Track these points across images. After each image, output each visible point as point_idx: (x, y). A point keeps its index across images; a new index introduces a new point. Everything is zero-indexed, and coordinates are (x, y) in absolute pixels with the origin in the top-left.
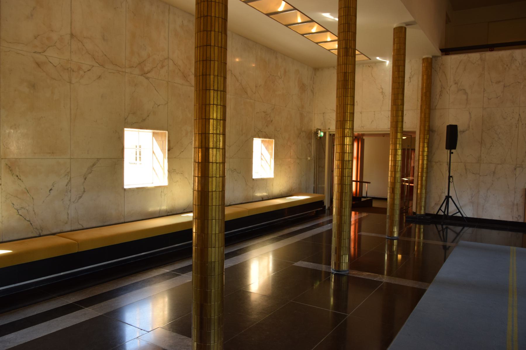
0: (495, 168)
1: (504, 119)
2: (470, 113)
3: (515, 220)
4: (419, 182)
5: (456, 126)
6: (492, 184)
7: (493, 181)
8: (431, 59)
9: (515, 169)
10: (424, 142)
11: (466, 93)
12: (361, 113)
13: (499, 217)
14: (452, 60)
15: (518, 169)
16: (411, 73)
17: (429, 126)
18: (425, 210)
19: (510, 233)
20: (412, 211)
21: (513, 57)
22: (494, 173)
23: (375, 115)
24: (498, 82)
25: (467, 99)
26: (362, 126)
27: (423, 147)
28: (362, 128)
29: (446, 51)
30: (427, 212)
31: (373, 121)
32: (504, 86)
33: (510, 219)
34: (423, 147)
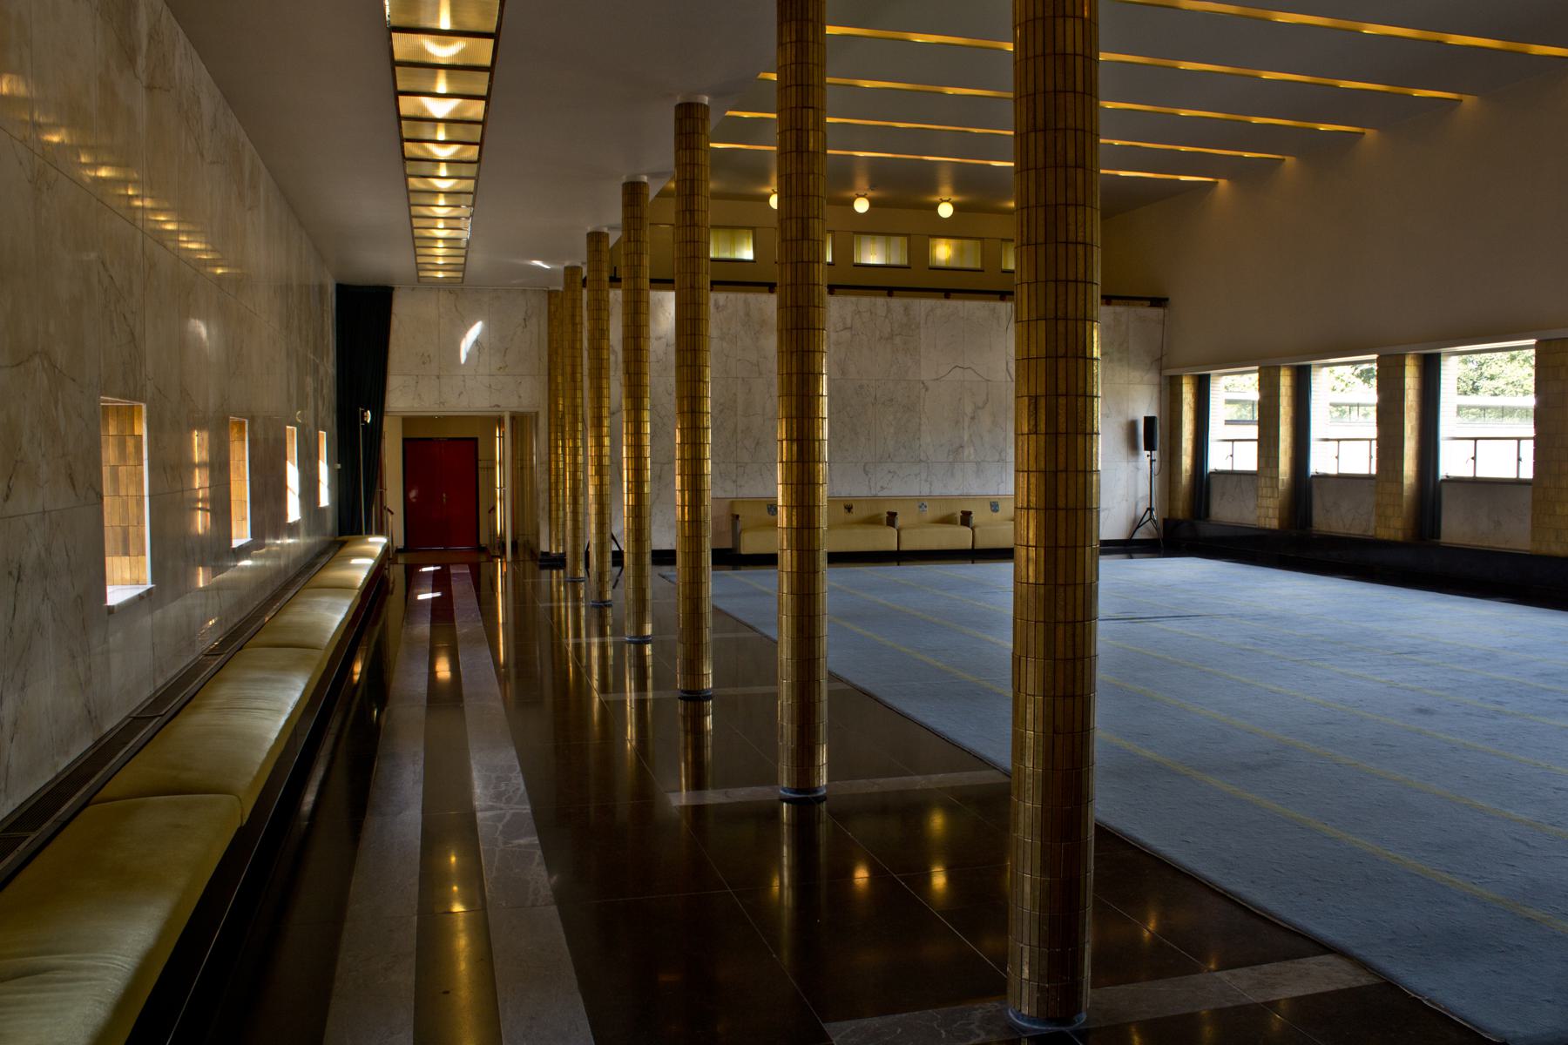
0: (661, 470)
4: (554, 499)
6: (658, 495)
7: (659, 490)
12: (438, 377)
13: (671, 544)
16: (526, 313)
20: (452, 564)
22: (660, 477)
23: (464, 381)
26: (441, 403)
28: (441, 405)
31: (462, 393)
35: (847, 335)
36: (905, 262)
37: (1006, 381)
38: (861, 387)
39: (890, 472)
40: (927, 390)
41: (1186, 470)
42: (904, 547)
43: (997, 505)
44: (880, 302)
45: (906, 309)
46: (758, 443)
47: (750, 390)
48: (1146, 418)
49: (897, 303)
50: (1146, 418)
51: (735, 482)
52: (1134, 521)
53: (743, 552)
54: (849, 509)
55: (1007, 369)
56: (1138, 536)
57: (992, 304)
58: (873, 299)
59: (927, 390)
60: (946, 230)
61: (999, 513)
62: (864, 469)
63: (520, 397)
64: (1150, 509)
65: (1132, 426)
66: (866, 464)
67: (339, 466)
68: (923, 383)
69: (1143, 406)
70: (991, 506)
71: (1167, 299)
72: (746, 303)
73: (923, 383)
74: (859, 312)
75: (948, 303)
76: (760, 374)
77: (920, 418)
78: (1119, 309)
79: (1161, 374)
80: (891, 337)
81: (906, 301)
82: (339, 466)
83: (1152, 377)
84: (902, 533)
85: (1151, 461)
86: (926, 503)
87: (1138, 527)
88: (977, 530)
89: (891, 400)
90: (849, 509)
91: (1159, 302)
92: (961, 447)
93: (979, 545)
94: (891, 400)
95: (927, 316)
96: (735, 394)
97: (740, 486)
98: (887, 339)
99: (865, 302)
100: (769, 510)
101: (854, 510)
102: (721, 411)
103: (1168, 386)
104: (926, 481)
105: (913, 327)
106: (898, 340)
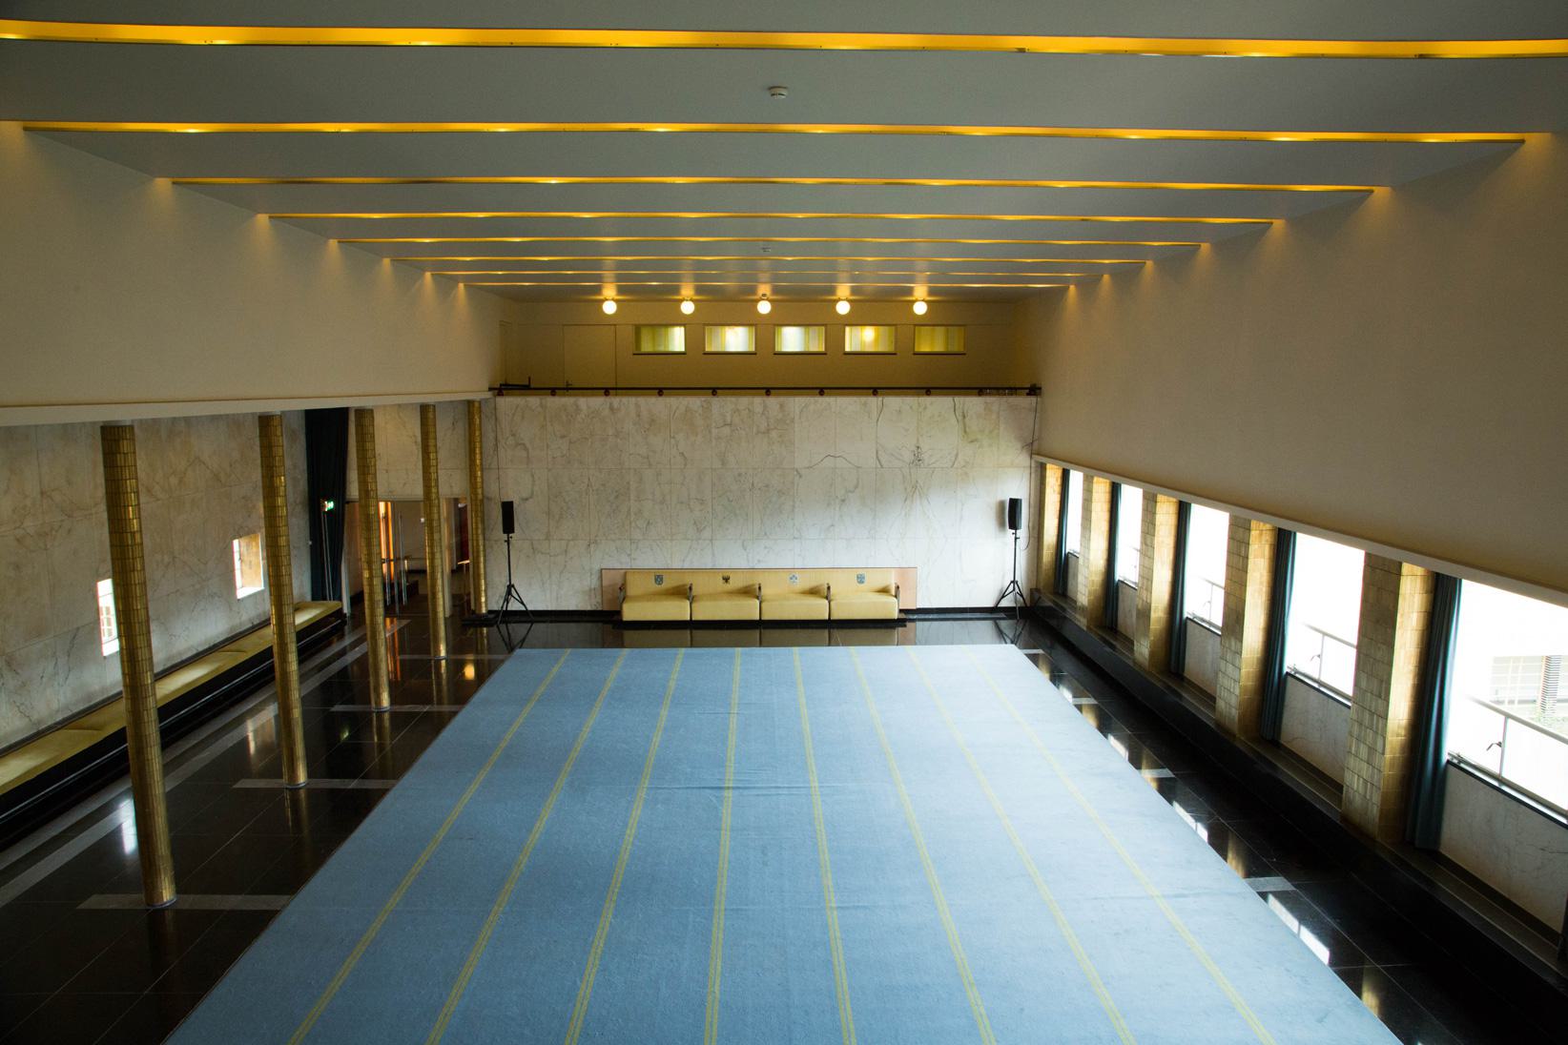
1: (573, 484)
2: (533, 476)
3: (594, 608)
5: (512, 503)
8: (480, 402)
9: (589, 545)
10: (476, 517)
11: (526, 449)
14: (507, 403)
15: (592, 546)
17: (483, 493)
18: (486, 606)
19: (589, 625)
21: (577, 406)
22: (566, 551)
24: (563, 437)
25: (528, 457)
27: (476, 523)
29: (502, 389)
30: (490, 608)
32: (570, 442)
33: (589, 608)
34: (476, 523)
35: (726, 430)
36: (822, 348)
37: (876, 468)
38: (740, 475)
39: (766, 548)
40: (801, 477)
41: (1048, 546)
42: (765, 617)
43: (864, 578)
44: (758, 401)
45: (782, 406)
46: (649, 523)
47: (641, 479)
48: (1011, 500)
49: (773, 401)
50: (1011, 500)
51: (629, 555)
52: (1001, 591)
53: (624, 619)
54: (726, 580)
55: (877, 457)
56: (1004, 603)
57: (863, 399)
58: (751, 399)
59: (801, 477)
60: (856, 320)
61: (862, 585)
62: (743, 545)
63: (451, 487)
64: (1014, 582)
65: (1002, 504)
66: (744, 541)
67: (310, 543)
68: (797, 471)
69: (1018, 487)
70: (858, 577)
71: (1040, 389)
72: (637, 406)
73: (797, 471)
74: (738, 410)
75: (820, 399)
76: (650, 465)
77: (794, 501)
78: (989, 399)
79: (1031, 458)
80: (768, 431)
81: (782, 399)
82: (310, 543)
83: (1024, 459)
84: (763, 605)
85: (1016, 538)
86: (797, 576)
87: (1003, 597)
88: (832, 603)
89: (767, 486)
90: (726, 580)
91: (1034, 391)
92: (832, 526)
93: (835, 616)
94: (767, 486)
95: (801, 412)
96: (628, 483)
97: (634, 559)
98: (764, 433)
99: (744, 401)
100: (656, 580)
101: (731, 581)
102: (617, 497)
103: (1039, 470)
104: (799, 555)
105: (788, 422)
106: (774, 434)
